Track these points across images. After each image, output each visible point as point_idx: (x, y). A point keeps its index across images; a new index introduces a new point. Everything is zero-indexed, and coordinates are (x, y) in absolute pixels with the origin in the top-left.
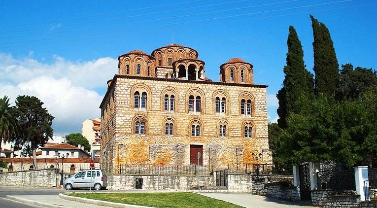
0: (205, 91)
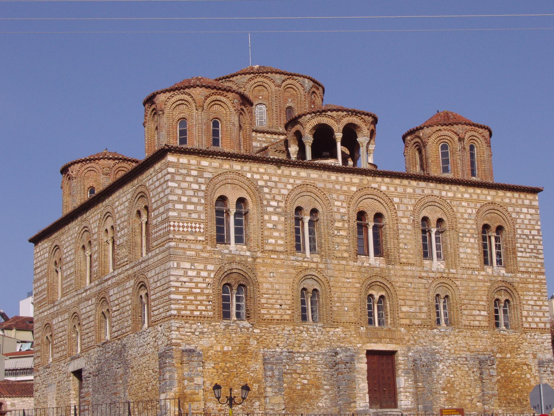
0: (396, 200)
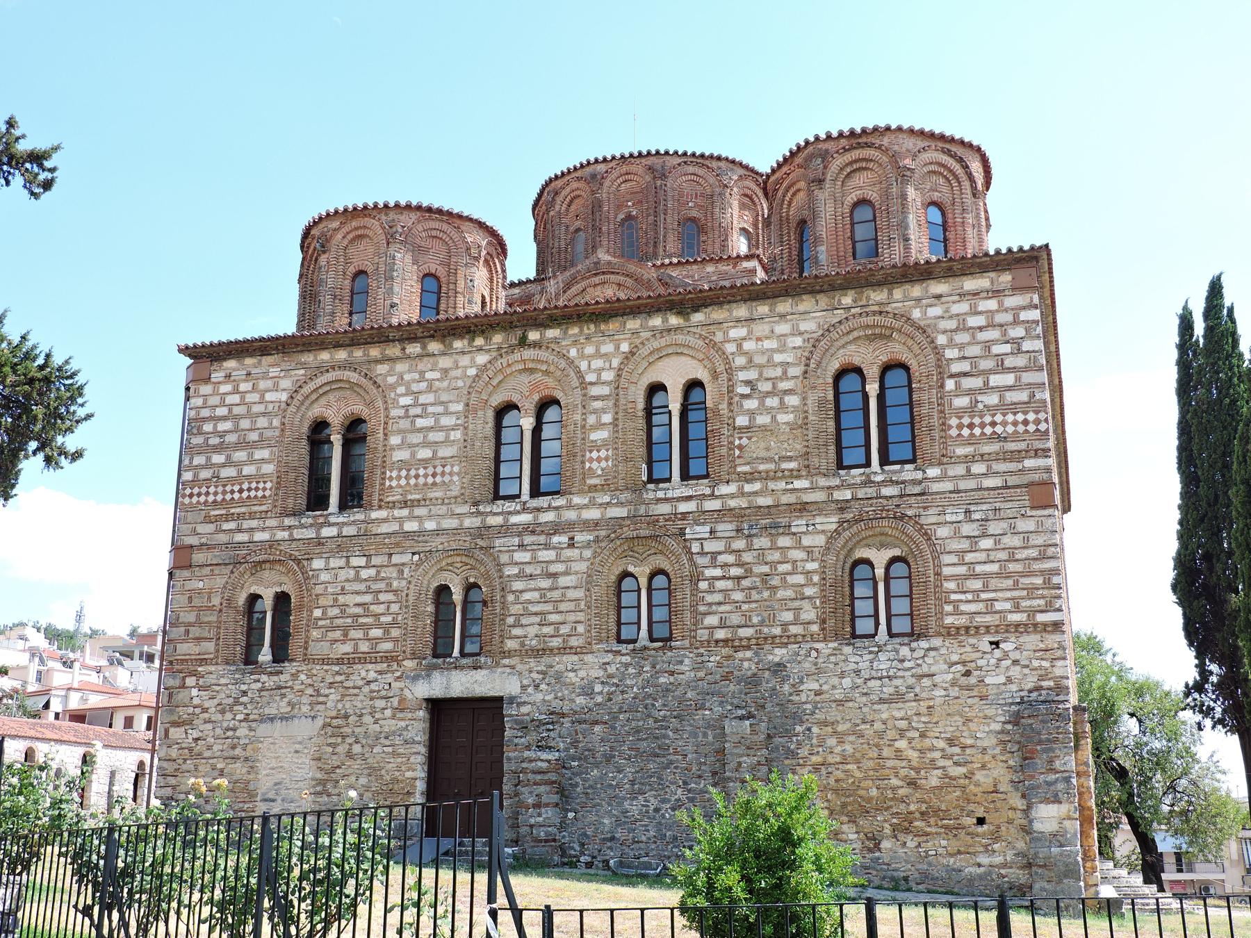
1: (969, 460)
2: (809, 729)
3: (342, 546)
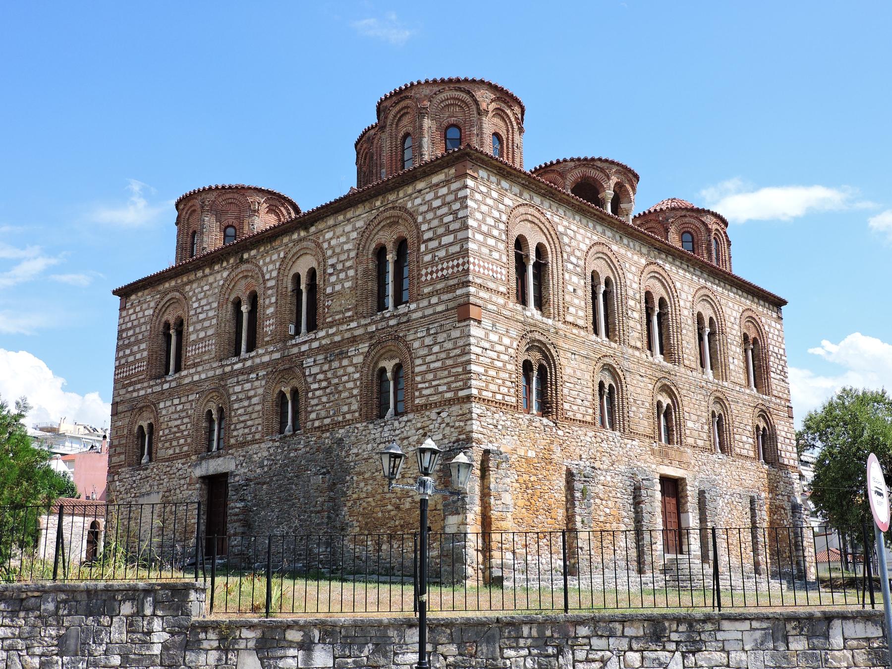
0: (678, 285)
1: (431, 295)
2: (352, 478)
3: (170, 394)
